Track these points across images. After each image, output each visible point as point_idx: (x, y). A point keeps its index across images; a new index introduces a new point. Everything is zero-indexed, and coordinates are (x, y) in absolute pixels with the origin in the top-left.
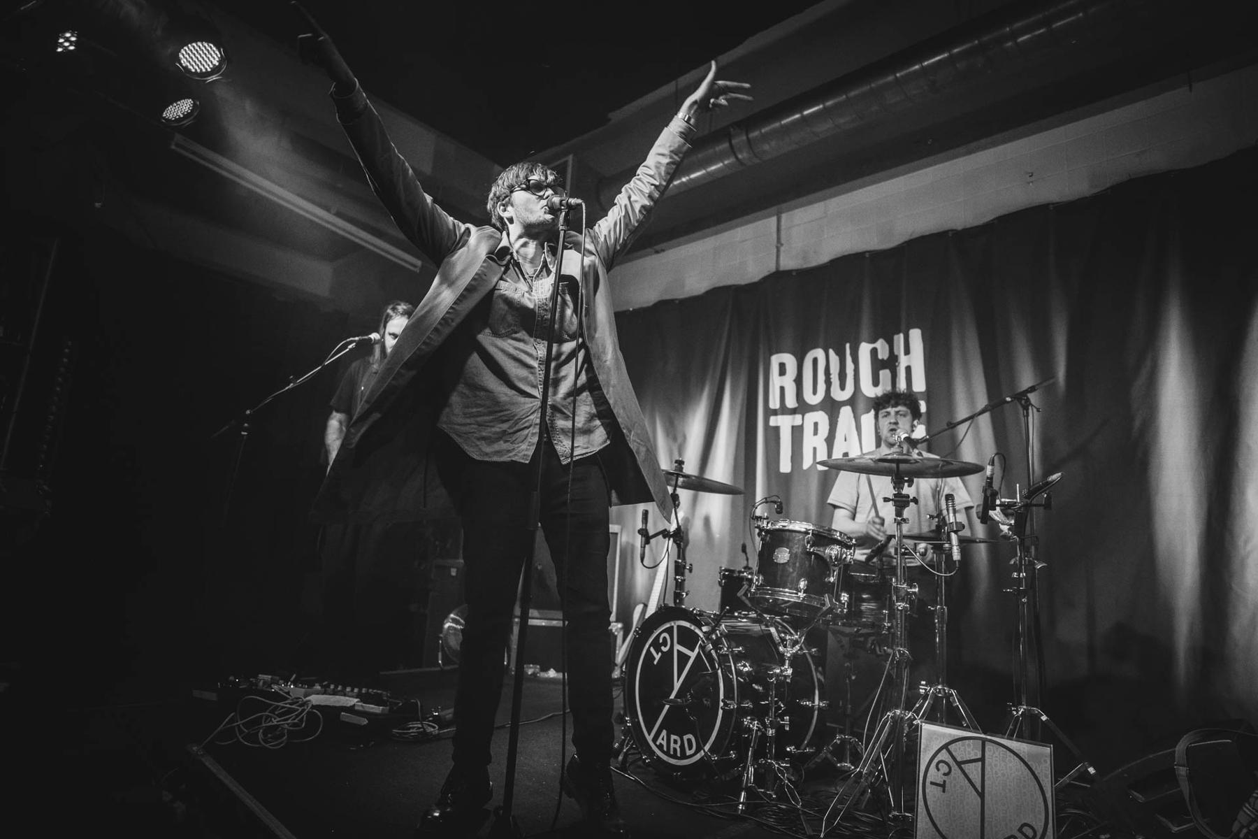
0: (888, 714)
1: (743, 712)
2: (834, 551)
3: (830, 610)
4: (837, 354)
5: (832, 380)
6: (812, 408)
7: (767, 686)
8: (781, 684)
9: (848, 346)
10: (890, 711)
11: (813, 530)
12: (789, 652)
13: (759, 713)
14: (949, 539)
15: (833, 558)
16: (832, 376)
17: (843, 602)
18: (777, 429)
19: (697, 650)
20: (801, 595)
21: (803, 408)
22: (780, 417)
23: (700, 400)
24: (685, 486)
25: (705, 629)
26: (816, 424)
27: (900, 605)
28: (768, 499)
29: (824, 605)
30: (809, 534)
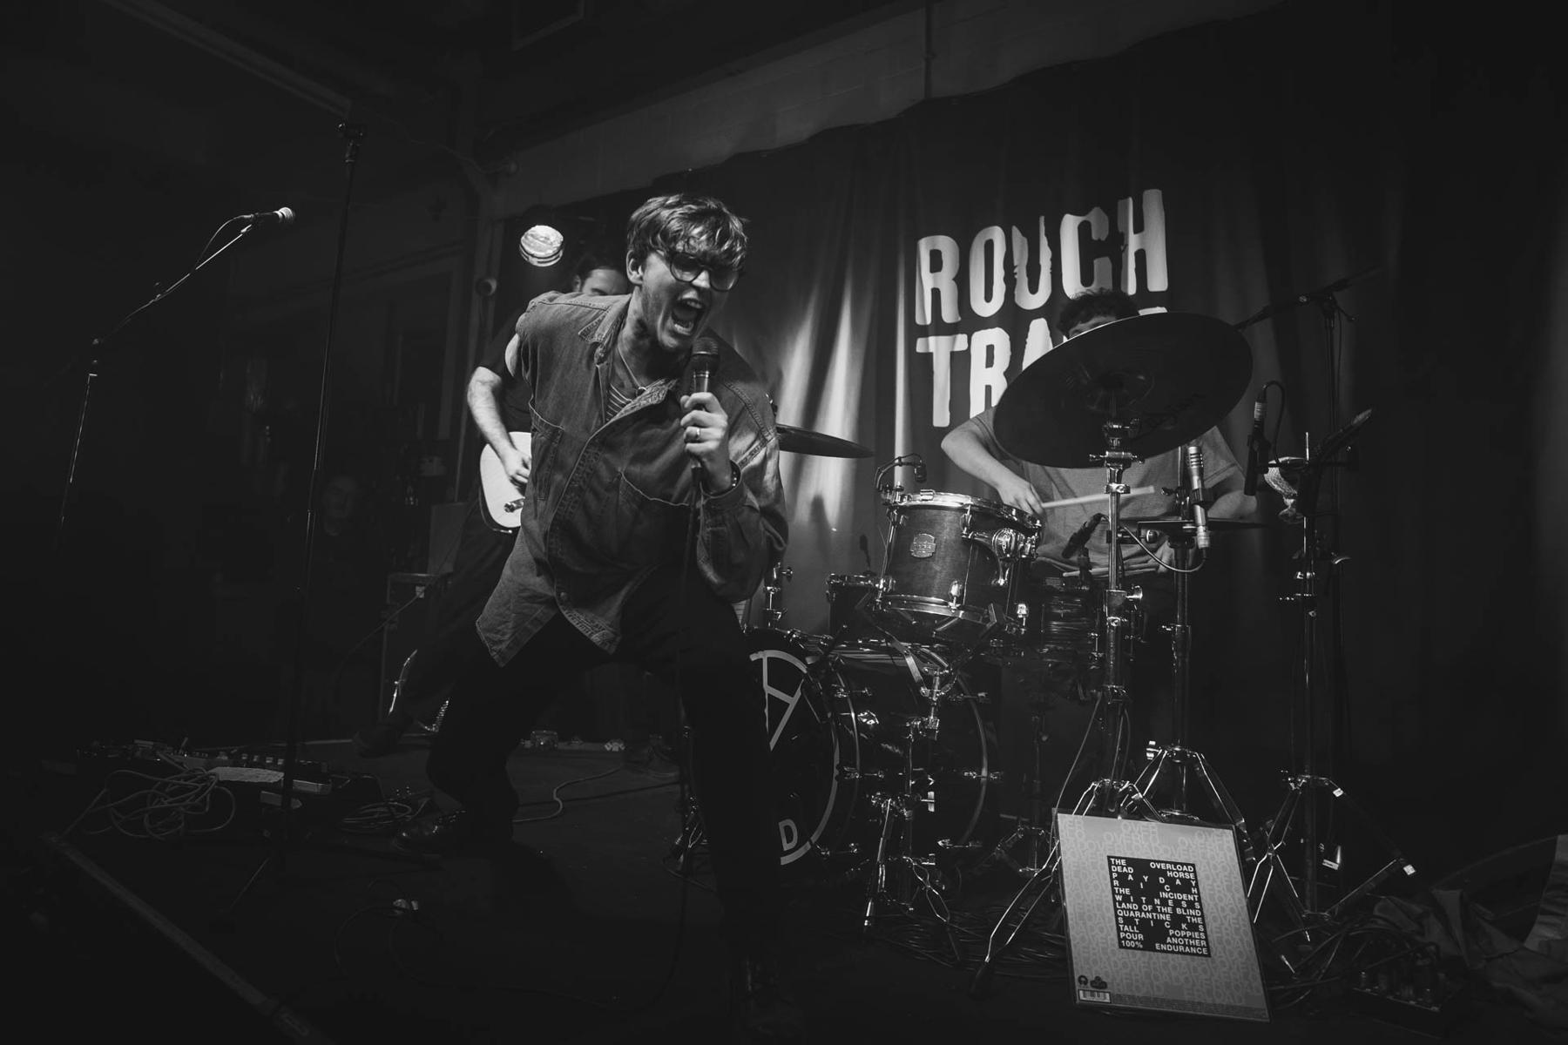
0: (1093, 784)
1: (870, 786)
2: (1005, 538)
3: (998, 631)
4: (1024, 234)
5: (1016, 277)
6: (985, 323)
7: (902, 744)
8: (924, 744)
9: (1042, 219)
10: (1096, 780)
11: (972, 505)
12: (937, 693)
13: (893, 787)
14: (1192, 517)
15: (1004, 548)
16: (1016, 271)
17: (1020, 616)
18: (928, 358)
19: (798, 693)
20: (953, 605)
21: (970, 323)
22: (932, 339)
23: (805, 308)
24: (783, 446)
25: (809, 661)
26: (990, 349)
27: (1113, 620)
28: (903, 460)
29: (987, 620)
30: (966, 511)
